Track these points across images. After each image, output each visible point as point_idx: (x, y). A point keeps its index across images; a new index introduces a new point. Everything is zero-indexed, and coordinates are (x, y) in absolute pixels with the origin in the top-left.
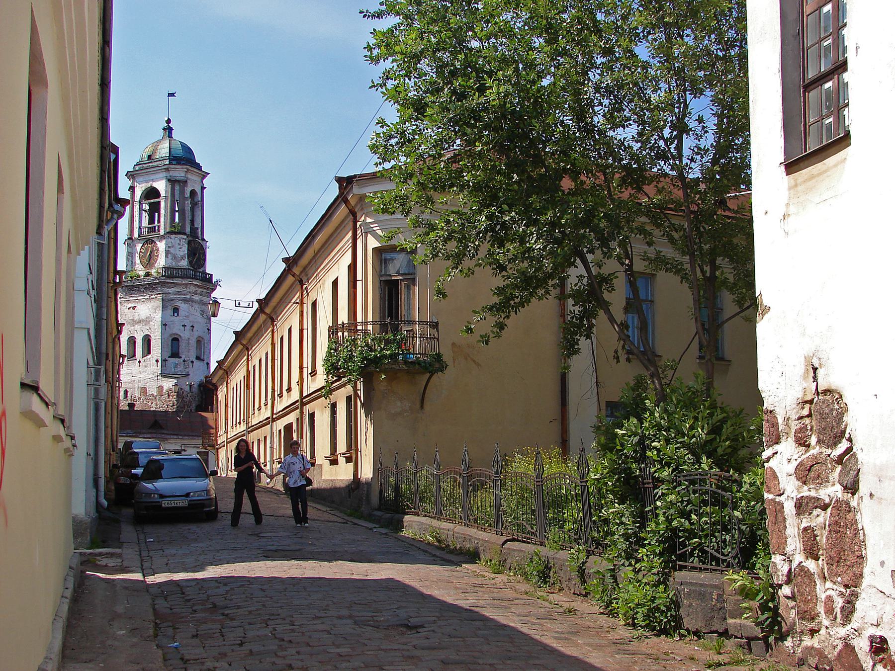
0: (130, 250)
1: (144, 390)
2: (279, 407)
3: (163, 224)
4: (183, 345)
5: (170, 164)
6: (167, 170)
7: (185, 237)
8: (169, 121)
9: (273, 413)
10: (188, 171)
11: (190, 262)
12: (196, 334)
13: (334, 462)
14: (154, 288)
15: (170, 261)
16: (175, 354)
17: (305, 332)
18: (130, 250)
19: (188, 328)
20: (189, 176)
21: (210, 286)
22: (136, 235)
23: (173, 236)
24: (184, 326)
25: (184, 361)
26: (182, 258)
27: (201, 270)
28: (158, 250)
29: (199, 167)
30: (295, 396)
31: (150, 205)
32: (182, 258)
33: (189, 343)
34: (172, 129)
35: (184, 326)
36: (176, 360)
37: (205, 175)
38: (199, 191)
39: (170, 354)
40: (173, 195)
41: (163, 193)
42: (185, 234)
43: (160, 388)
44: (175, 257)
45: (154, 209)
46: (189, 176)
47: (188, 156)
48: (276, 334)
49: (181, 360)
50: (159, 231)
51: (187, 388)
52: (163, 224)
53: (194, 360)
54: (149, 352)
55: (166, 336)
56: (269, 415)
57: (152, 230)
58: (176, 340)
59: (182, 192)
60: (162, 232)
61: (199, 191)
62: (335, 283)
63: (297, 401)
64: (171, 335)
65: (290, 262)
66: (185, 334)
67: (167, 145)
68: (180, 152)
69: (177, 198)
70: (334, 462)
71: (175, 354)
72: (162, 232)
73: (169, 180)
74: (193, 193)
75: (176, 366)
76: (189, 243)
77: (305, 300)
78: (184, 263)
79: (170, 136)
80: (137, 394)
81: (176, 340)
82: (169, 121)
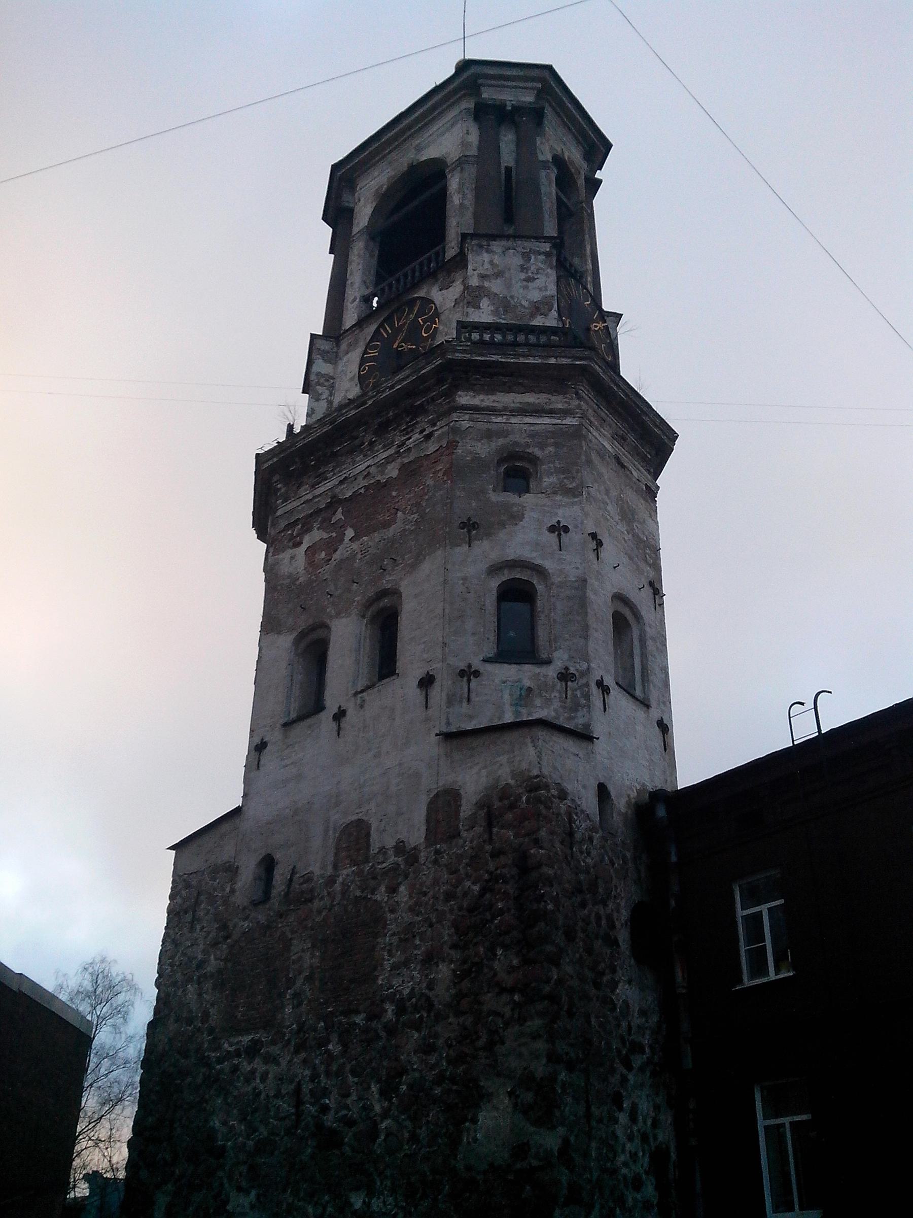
1: (355, 838)
4: (551, 607)
7: (547, 247)
19: (574, 538)
25: (565, 676)
33: (582, 603)
35: (558, 529)
36: (526, 674)
39: (490, 649)
42: (539, 238)
43: (445, 802)
49: (551, 672)
51: (589, 802)
58: (517, 593)
59: (525, 146)
64: (495, 569)
66: (563, 564)
75: (525, 696)
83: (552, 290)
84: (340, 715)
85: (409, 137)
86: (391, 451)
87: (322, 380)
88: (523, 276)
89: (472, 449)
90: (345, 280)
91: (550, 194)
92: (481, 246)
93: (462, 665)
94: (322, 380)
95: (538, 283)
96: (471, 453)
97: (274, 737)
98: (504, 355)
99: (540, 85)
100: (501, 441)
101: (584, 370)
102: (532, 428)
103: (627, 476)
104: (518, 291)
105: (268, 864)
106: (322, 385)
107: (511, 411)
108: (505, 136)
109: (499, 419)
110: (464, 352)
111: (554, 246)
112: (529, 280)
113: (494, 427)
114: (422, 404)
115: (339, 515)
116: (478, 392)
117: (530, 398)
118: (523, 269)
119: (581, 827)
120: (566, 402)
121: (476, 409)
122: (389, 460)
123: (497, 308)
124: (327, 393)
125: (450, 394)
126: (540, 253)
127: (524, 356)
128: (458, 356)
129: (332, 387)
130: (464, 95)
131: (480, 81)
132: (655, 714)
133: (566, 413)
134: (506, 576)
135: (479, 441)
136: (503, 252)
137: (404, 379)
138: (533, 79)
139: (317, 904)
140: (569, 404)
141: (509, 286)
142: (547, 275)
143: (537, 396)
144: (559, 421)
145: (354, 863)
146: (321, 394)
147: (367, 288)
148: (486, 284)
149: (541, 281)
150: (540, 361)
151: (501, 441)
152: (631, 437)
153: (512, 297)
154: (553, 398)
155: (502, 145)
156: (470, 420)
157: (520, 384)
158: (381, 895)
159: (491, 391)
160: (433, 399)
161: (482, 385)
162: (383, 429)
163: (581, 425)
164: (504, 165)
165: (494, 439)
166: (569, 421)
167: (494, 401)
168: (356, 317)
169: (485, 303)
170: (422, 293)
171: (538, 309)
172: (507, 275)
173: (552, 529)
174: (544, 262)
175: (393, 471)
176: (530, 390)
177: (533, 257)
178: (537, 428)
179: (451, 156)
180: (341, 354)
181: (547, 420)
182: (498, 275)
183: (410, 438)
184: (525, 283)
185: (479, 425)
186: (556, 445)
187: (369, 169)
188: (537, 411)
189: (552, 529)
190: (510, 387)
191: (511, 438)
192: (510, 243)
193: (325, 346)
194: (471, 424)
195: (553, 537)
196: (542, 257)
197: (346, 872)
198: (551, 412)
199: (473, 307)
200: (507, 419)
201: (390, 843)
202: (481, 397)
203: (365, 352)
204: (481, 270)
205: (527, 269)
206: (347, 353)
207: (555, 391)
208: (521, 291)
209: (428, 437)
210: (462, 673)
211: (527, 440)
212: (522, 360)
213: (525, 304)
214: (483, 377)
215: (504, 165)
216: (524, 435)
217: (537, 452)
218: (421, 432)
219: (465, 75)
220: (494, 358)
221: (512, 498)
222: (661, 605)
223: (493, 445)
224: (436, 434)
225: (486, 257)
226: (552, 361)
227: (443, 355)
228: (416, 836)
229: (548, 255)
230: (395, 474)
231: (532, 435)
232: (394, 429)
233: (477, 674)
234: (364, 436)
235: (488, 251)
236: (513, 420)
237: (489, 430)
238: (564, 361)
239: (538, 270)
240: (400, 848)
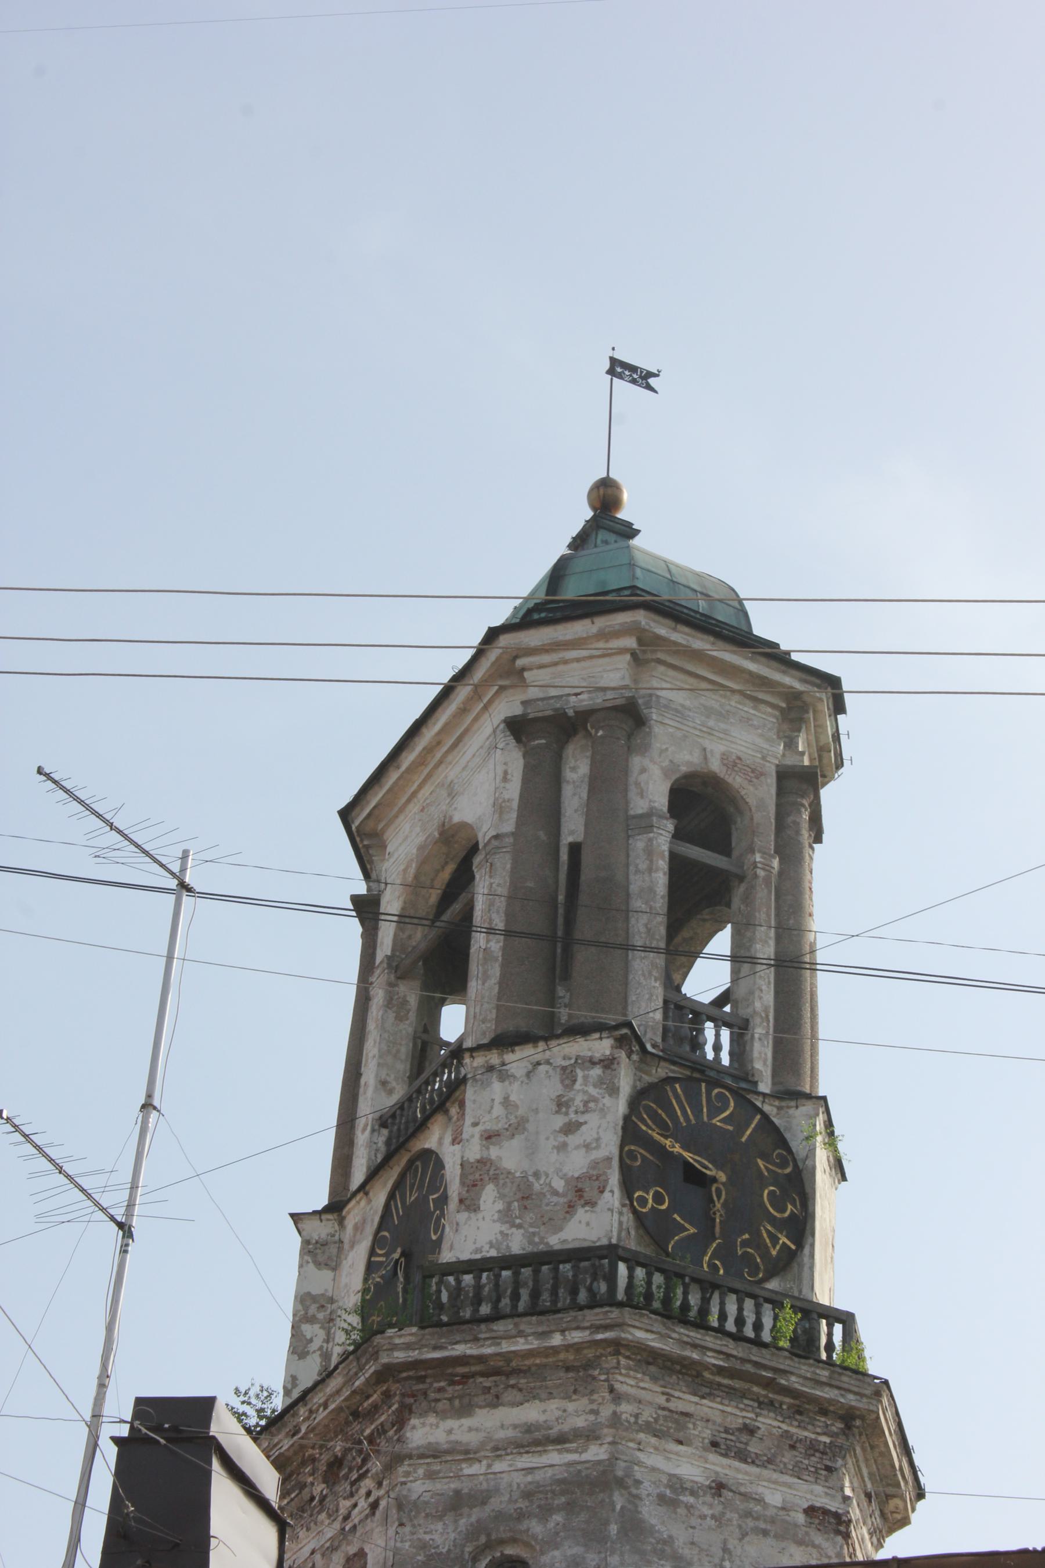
0: (322, 1282)
6: (511, 673)
7: (601, 1046)
8: (605, 497)
10: (637, 660)
18: (322, 1282)
23: (518, 1059)
26: (581, 1193)
32: (581, 1193)
34: (629, 532)
38: (760, 796)
61: (760, 796)
69: (573, 827)
82: (605, 497)
83: (610, 1144)
85: (440, 762)
87: (313, 1309)
88: (559, 1121)
89: (427, 1537)
90: (359, 1075)
91: (651, 890)
92: (490, 1069)
94: (313, 1309)
95: (586, 1134)
96: (424, 1546)
98: (476, 1339)
99: (631, 642)
100: (476, 1514)
101: (617, 1346)
102: (529, 1478)
103: (748, 1514)
104: (548, 1160)
106: (310, 1320)
107: (496, 1449)
108: (574, 769)
109: (475, 1469)
110: (408, 1347)
112: (570, 1128)
113: (465, 1487)
114: (372, 1433)
116: (443, 1415)
117: (532, 1413)
118: (561, 1105)
120: (593, 1412)
121: (434, 1453)
123: (509, 1204)
124: (322, 1334)
125: (400, 1422)
126: (592, 1062)
127: (508, 1337)
128: (400, 1356)
130: (502, 688)
131: (520, 663)
133: (590, 1435)
135: (440, 1518)
136: (528, 1075)
137: (338, 1392)
138: (617, 634)
140: (595, 1412)
141: (531, 1151)
142: (602, 1110)
143: (542, 1406)
144: (575, 1457)
146: (311, 1341)
147: (390, 1092)
148: (494, 1152)
150: (534, 1344)
151: (476, 1514)
152: (768, 1422)
153: (537, 1175)
154: (571, 1407)
155: (567, 791)
156: (431, 1476)
157: (513, 1386)
159: (465, 1410)
160: (382, 1431)
161: (450, 1399)
163: (613, 1459)
164: (567, 839)
165: (466, 1510)
166: (596, 1452)
167: (470, 1429)
168: (365, 1170)
171: (579, 1191)
172: (531, 1127)
174: (600, 1083)
176: (532, 1396)
177: (580, 1073)
178: (538, 1476)
179: (484, 829)
180: (346, 1246)
181: (554, 1457)
182: (518, 1127)
183: (355, 1505)
184: (562, 1138)
185: (439, 1486)
186: (570, 1508)
187: (396, 816)
188: (537, 1443)
190: (497, 1397)
191: (496, 1503)
194: (428, 1485)
196: (597, 1071)
198: (561, 1440)
199: (468, 1209)
200: (489, 1466)
202: (451, 1423)
203: (372, 1253)
204: (488, 1124)
205: (567, 1105)
206: (352, 1247)
207: (575, 1392)
208: (554, 1157)
209: (374, 1506)
211: (522, 1504)
212: (506, 1347)
213: (559, 1184)
214: (453, 1383)
215: (567, 839)
216: (516, 1495)
217: (536, 1528)
218: (369, 1494)
219: (493, 655)
220: (460, 1349)
223: (463, 1522)
224: (383, 1503)
225: (497, 1089)
226: (557, 1340)
227: (375, 1356)
229: (608, 1063)
231: (528, 1495)
232: (346, 1477)
234: (312, 1484)
235: (504, 1076)
236: (499, 1466)
237: (457, 1493)
238: (576, 1336)
239: (586, 1103)
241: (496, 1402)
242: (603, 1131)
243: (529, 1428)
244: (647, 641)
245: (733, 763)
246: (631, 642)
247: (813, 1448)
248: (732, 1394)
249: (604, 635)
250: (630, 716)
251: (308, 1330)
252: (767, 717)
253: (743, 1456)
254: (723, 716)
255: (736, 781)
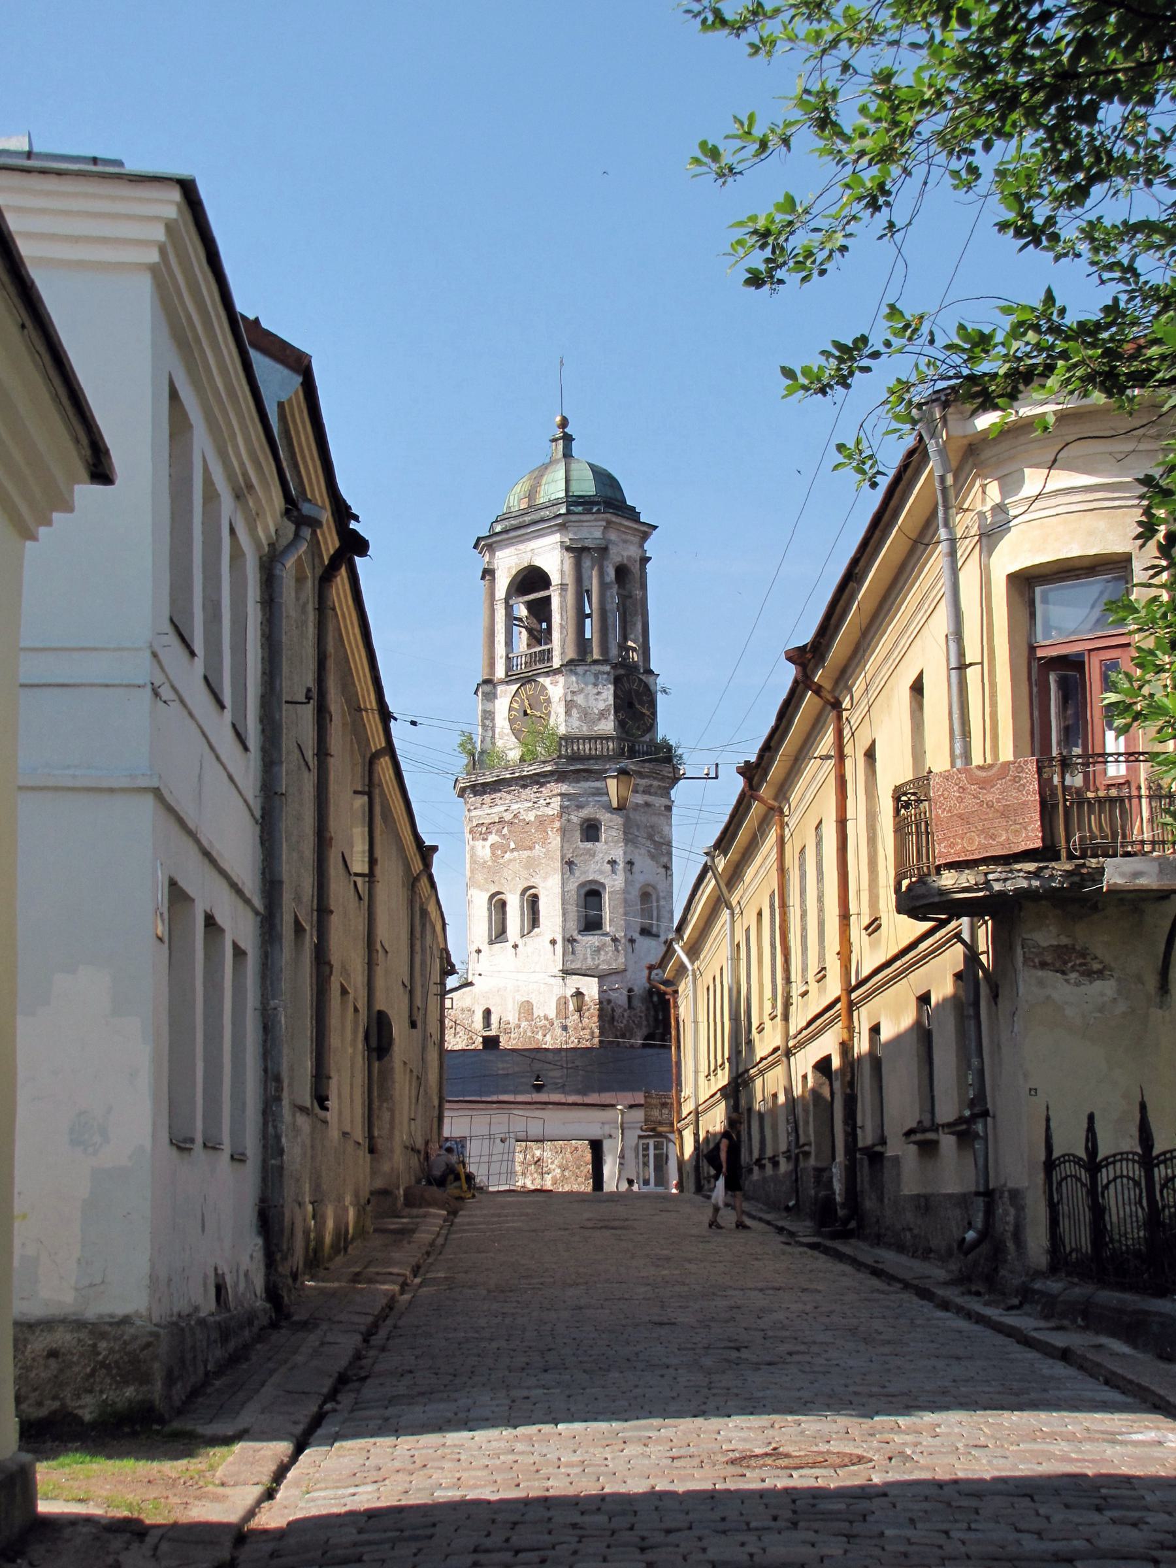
1: (527, 1009)
2: (798, 1021)
3: (560, 646)
5: (569, 512)
6: (563, 527)
7: (607, 668)
9: (787, 1037)
11: (621, 724)
12: (640, 879)
13: (928, 1149)
14: (542, 785)
15: (576, 723)
16: (592, 924)
17: (850, 825)
20: (613, 536)
21: (666, 771)
22: (500, 673)
24: (613, 863)
26: (602, 715)
27: (647, 738)
28: (548, 701)
29: (632, 514)
30: (834, 988)
31: (530, 605)
35: (613, 863)
37: (646, 531)
38: (635, 568)
40: (579, 579)
41: (555, 579)
44: (585, 714)
45: (540, 610)
46: (613, 536)
47: (609, 493)
48: (788, 847)
50: (550, 659)
52: (560, 646)
53: (636, 936)
54: (535, 922)
55: (573, 886)
56: (778, 1041)
57: (533, 659)
58: (592, 895)
60: (556, 663)
62: (917, 688)
63: (838, 1000)
65: (806, 658)
67: (561, 474)
68: (586, 486)
70: (928, 1149)
71: (592, 924)
72: (556, 663)
73: (568, 549)
74: (622, 572)
75: (598, 950)
76: (617, 681)
77: (848, 750)
78: (608, 726)
79: (567, 455)
80: (512, 1017)
81: (592, 895)
83: (611, 701)
84: (515, 946)
86: (530, 804)
88: (595, 691)
93: (567, 936)
97: (485, 947)
104: (592, 703)
105: (487, 1013)
111: (613, 668)
112: (598, 693)
115: (505, 831)
119: (618, 1011)
122: (528, 809)
129: (493, 719)
132: (662, 939)
134: (587, 888)
139: (512, 1035)
145: (527, 1020)
149: (604, 696)
152: (656, 783)
158: (540, 1036)
162: (524, 787)
169: (574, 712)
170: (541, 680)
173: (609, 862)
175: (531, 817)
182: (581, 691)
189: (609, 862)
192: (586, 668)
193: (487, 688)
195: (609, 867)
197: (524, 1024)
201: (542, 1015)
210: (568, 940)
221: (589, 845)
222: (671, 875)
228: (552, 1014)
229: (608, 673)
230: (532, 819)
233: (575, 940)
235: (576, 674)
240: (546, 1018)
241: (587, 780)
242: (607, 696)
243: (597, 789)
244: (609, 522)
245: (629, 557)
246: (604, 523)
247: (665, 788)
248: (648, 777)
249: (596, 520)
250: (604, 550)
251: (487, 722)
252: (636, 540)
253: (650, 794)
254: (625, 541)
255: (629, 564)
